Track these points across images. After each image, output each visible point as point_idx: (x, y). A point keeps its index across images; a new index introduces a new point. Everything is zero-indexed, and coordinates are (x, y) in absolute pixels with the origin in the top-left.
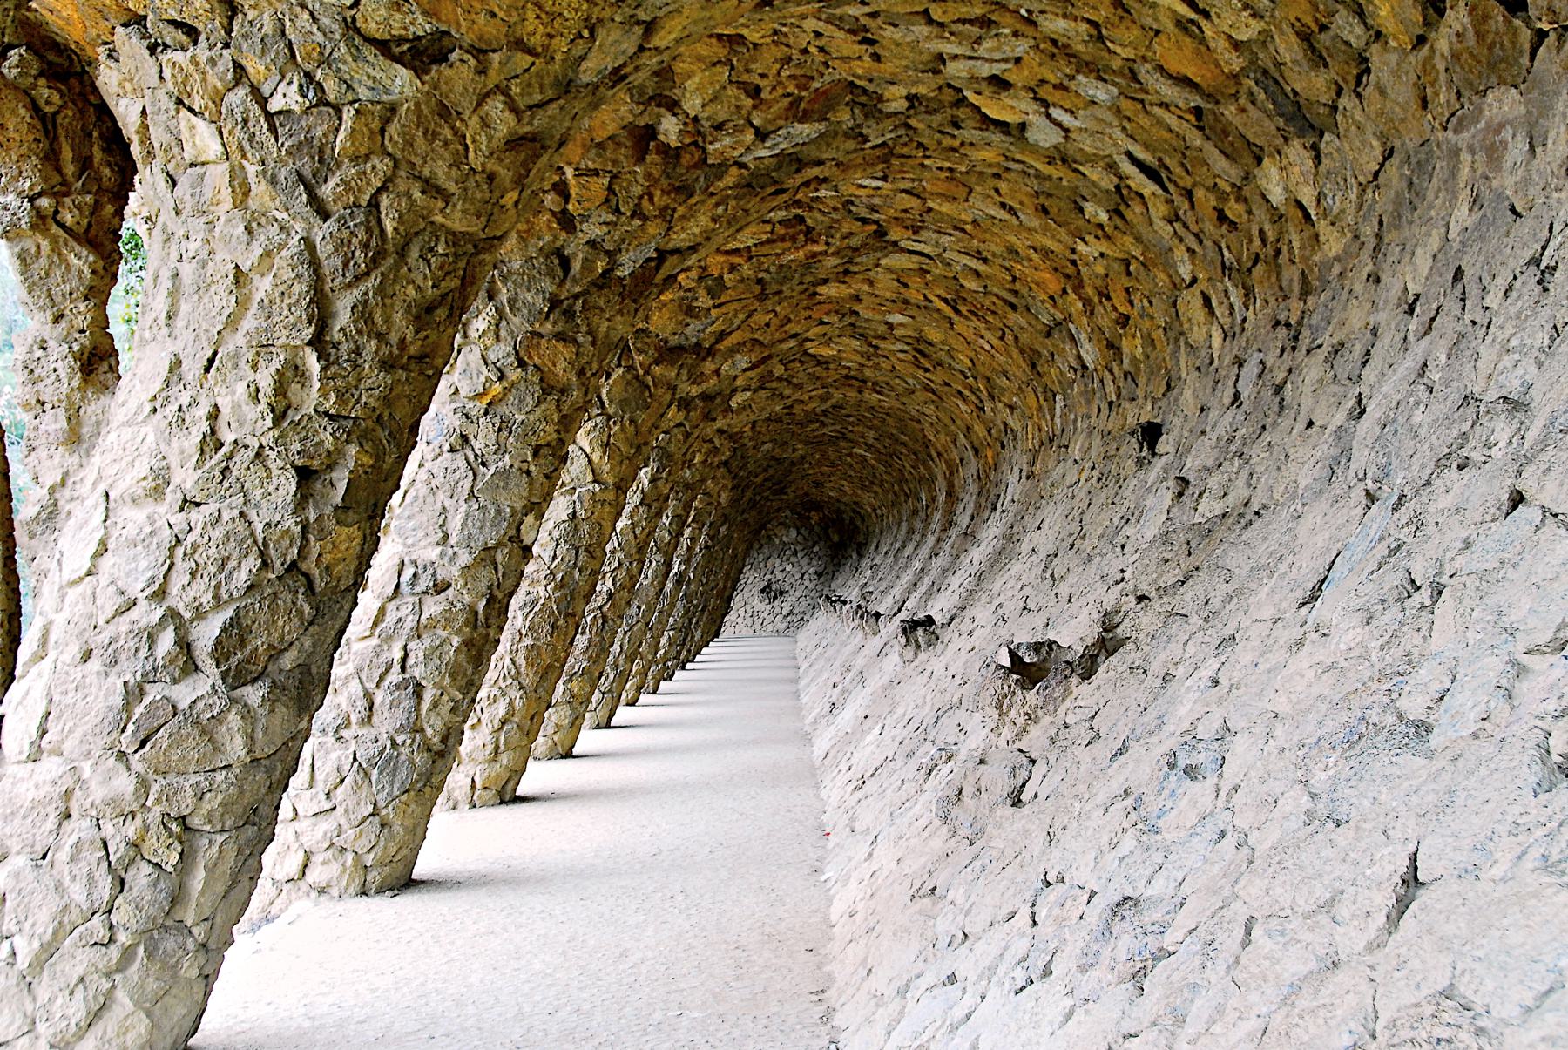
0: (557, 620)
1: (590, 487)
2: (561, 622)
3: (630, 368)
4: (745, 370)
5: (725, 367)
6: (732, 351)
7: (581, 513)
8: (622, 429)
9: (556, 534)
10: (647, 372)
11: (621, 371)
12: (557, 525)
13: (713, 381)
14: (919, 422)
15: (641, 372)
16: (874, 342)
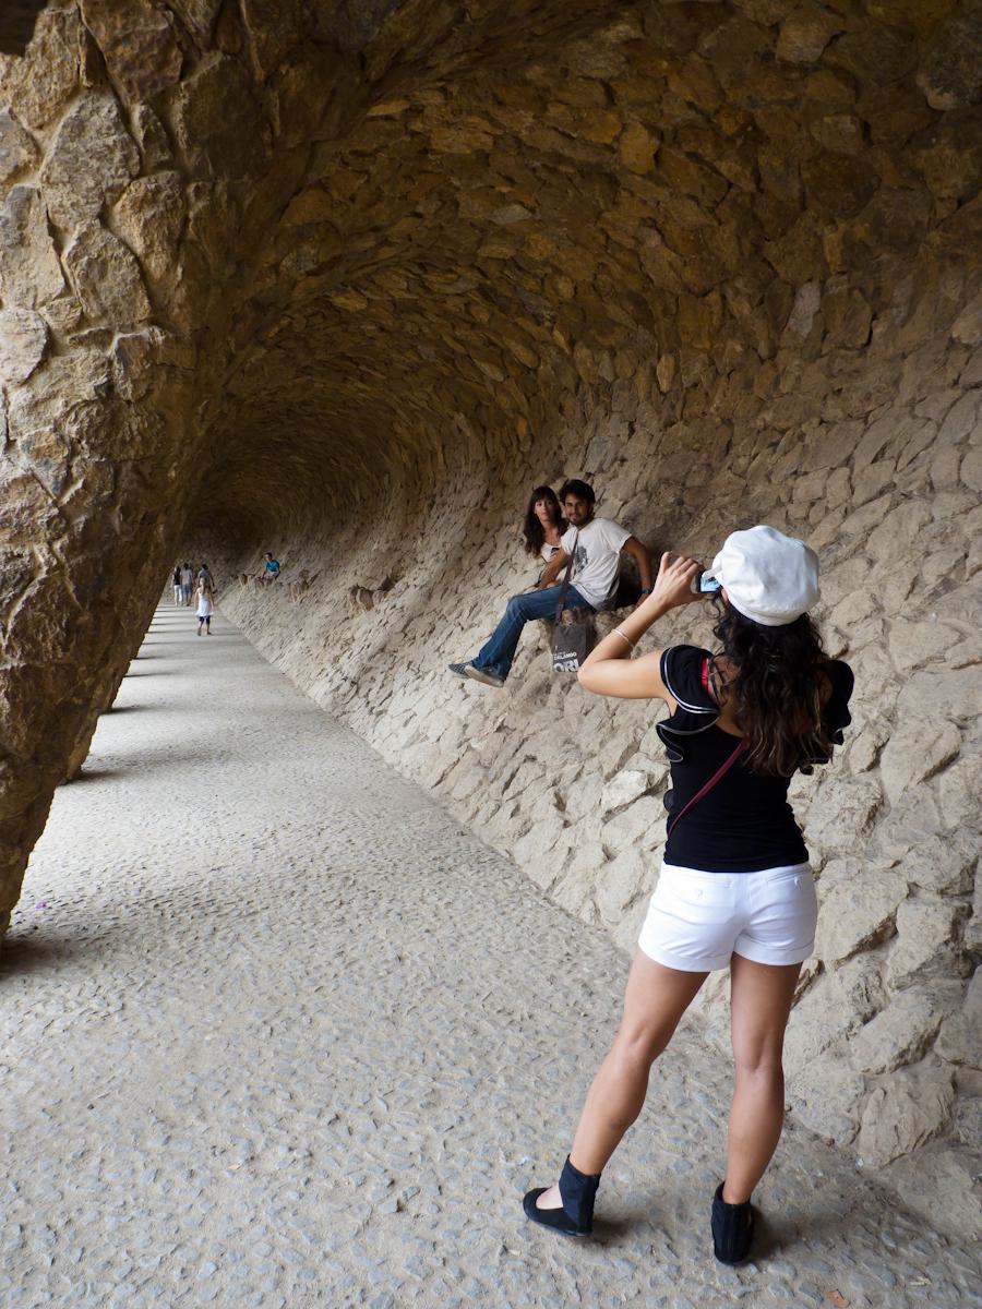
0: (76, 614)
1: (144, 332)
2: (85, 618)
3: (237, 56)
4: (309, 274)
5: (287, 262)
6: (301, 236)
7: (126, 389)
8: (212, 209)
9: (71, 430)
10: (271, 79)
11: (216, 59)
12: (71, 409)
13: (270, 281)
14: (393, 411)
15: (260, 75)
16: (432, 278)
